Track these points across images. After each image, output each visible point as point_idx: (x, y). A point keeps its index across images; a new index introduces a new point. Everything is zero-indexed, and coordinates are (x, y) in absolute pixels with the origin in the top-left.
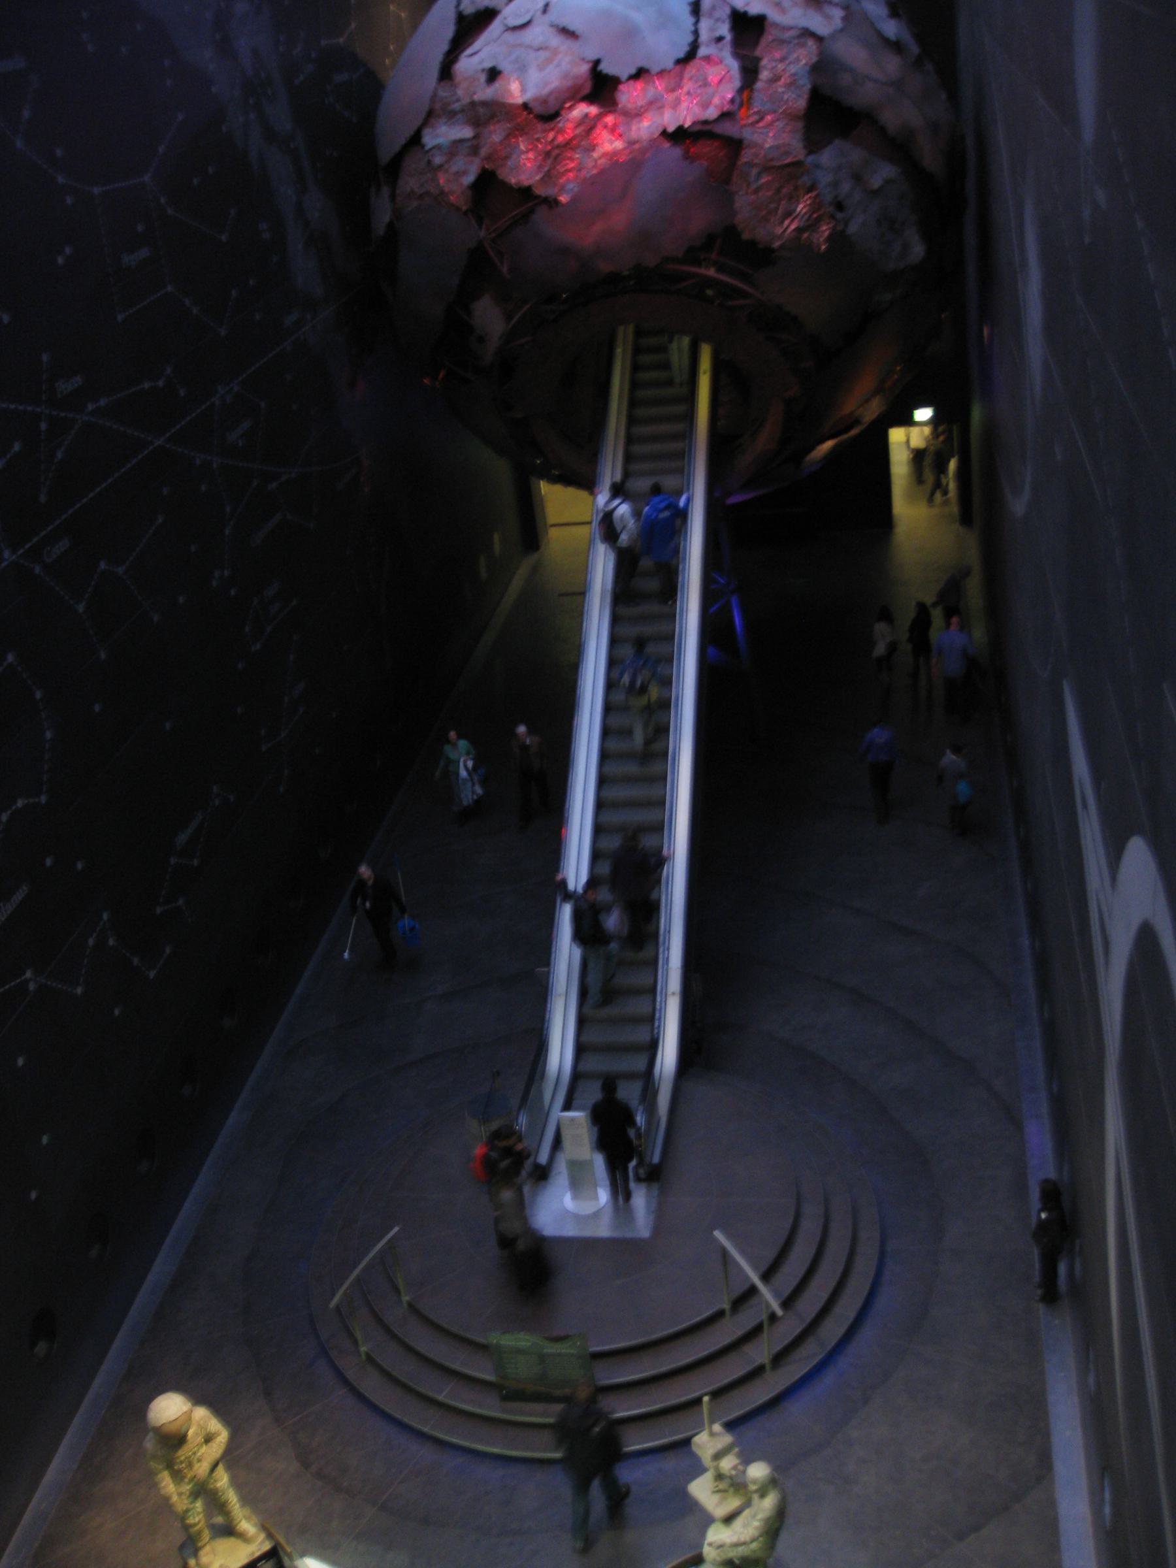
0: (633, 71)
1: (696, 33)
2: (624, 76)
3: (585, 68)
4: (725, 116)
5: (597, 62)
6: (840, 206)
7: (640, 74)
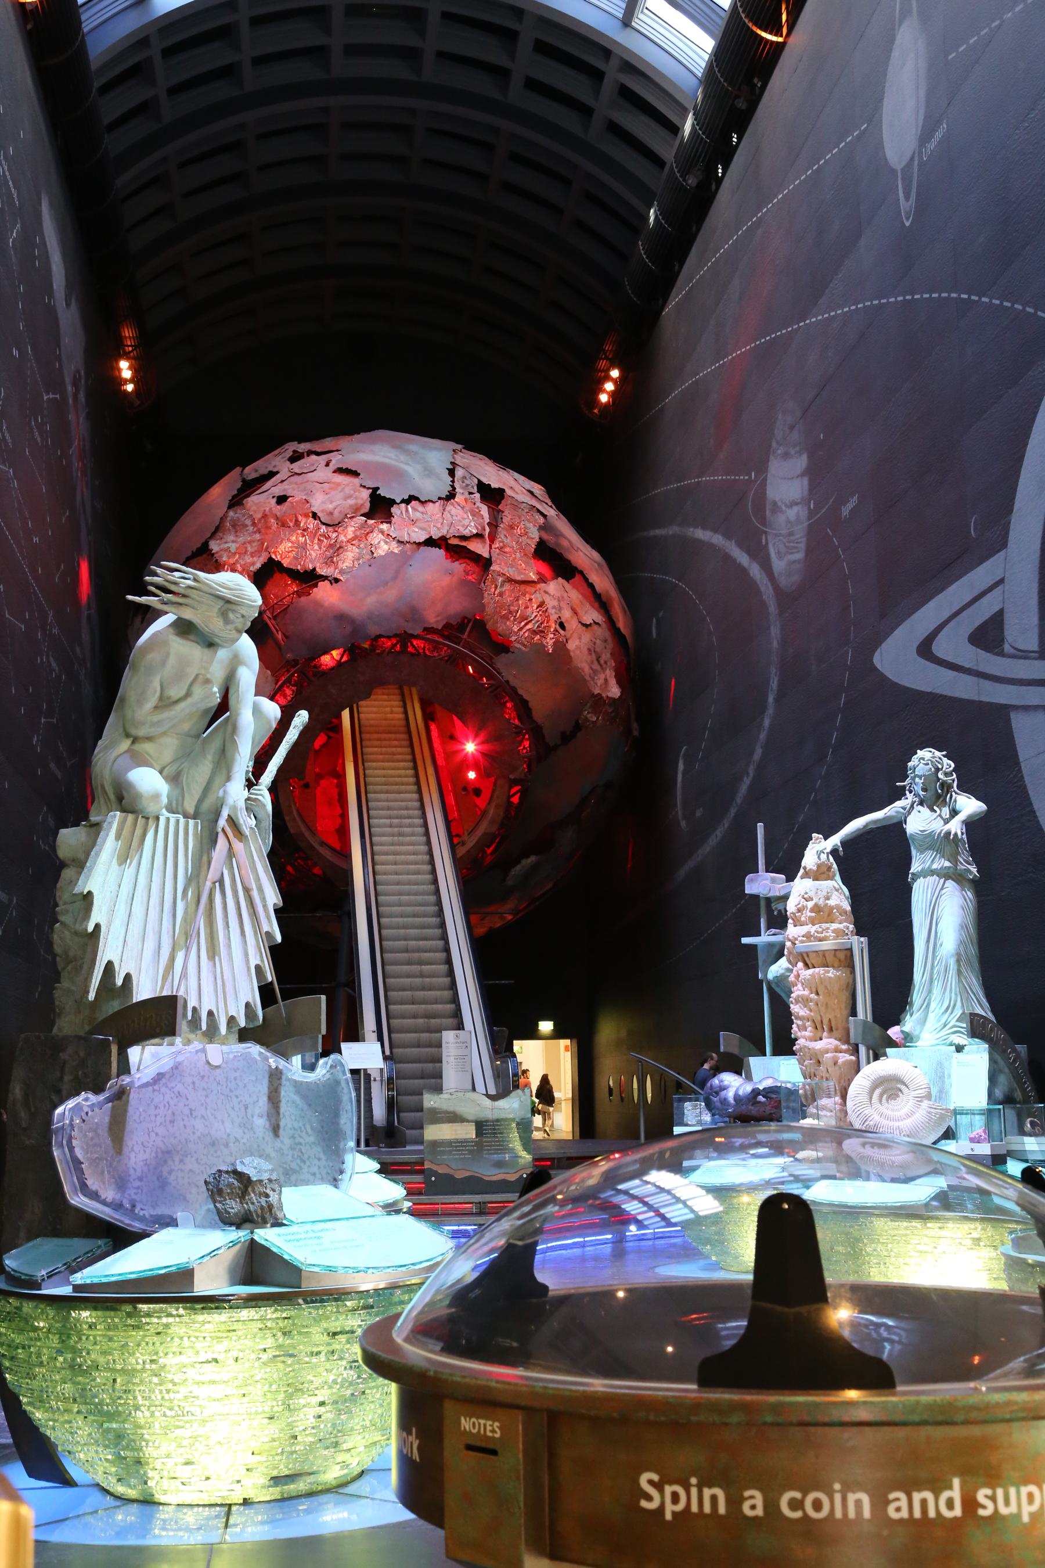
0: (406, 497)
1: (453, 486)
2: (398, 501)
3: (366, 494)
4: (479, 536)
5: (376, 489)
6: (562, 626)
7: (411, 499)
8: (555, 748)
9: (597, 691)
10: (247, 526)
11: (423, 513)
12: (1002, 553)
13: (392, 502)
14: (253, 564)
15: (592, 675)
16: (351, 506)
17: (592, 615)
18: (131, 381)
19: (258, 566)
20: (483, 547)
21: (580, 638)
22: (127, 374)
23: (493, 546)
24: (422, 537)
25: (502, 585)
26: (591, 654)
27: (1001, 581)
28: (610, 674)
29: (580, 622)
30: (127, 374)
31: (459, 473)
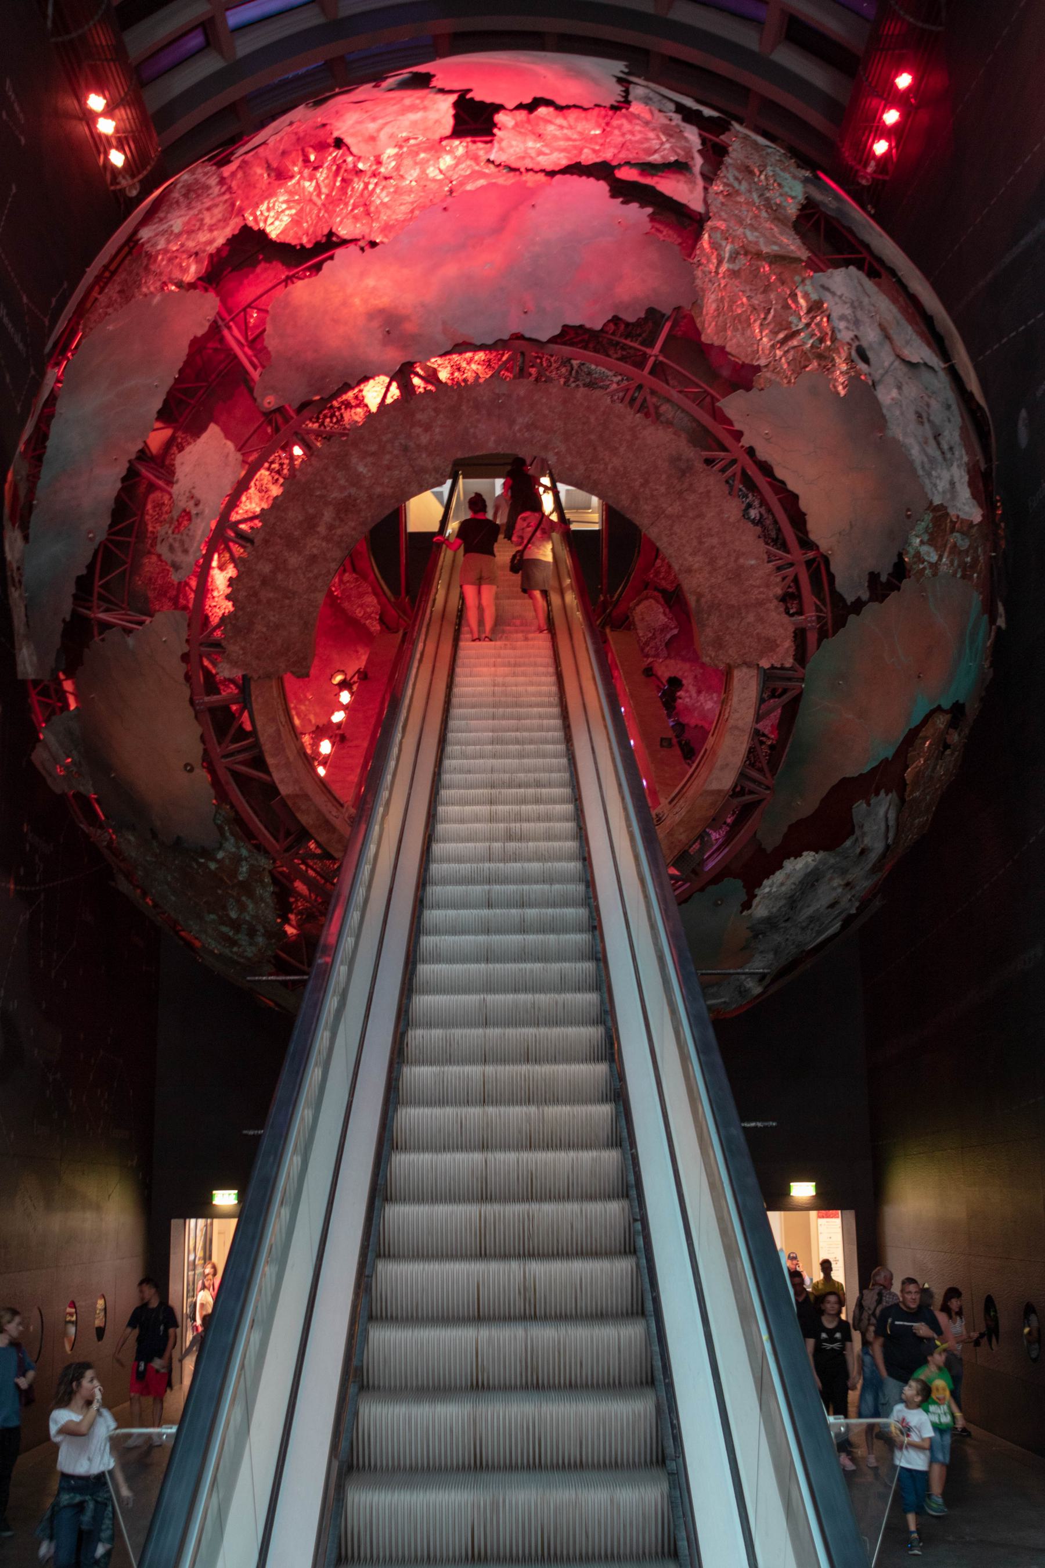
0: (527, 100)
2: (510, 105)
4: (679, 168)
8: (858, 606)
9: (937, 501)
10: (208, 187)
11: (561, 127)
13: (499, 108)
14: (211, 242)
15: (927, 466)
17: (920, 352)
19: (220, 241)
20: (691, 191)
21: (899, 388)
23: (710, 190)
25: (733, 259)
26: (922, 423)
28: (959, 475)
29: (898, 356)
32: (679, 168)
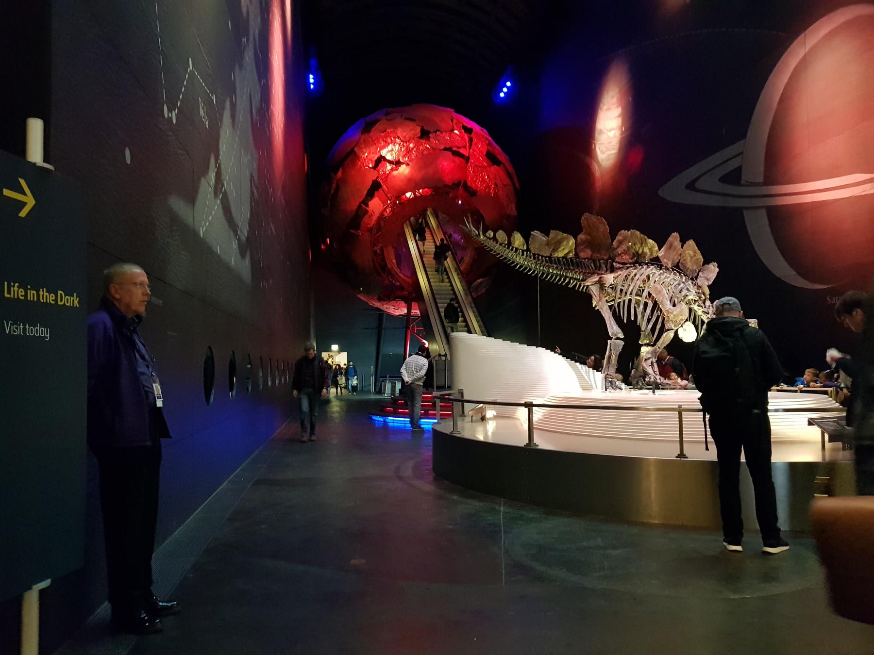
0: (435, 130)
2: (432, 131)
12: (742, 141)
13: (430, 132)
16: (413, 134)
18: (313, 84)
22: (312, 81)
24: (442, 147)
27: (742, 153)
30: (312, 81)
31: (455, 121)
32: (465, 147)
